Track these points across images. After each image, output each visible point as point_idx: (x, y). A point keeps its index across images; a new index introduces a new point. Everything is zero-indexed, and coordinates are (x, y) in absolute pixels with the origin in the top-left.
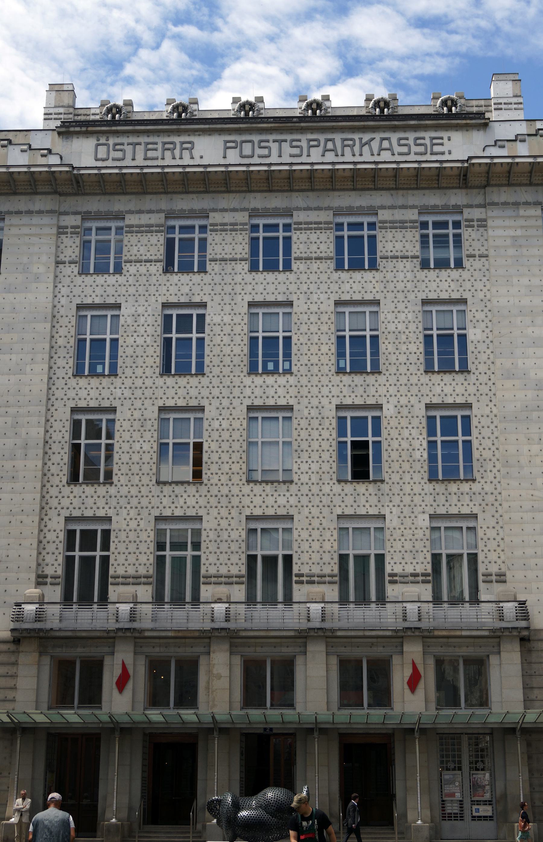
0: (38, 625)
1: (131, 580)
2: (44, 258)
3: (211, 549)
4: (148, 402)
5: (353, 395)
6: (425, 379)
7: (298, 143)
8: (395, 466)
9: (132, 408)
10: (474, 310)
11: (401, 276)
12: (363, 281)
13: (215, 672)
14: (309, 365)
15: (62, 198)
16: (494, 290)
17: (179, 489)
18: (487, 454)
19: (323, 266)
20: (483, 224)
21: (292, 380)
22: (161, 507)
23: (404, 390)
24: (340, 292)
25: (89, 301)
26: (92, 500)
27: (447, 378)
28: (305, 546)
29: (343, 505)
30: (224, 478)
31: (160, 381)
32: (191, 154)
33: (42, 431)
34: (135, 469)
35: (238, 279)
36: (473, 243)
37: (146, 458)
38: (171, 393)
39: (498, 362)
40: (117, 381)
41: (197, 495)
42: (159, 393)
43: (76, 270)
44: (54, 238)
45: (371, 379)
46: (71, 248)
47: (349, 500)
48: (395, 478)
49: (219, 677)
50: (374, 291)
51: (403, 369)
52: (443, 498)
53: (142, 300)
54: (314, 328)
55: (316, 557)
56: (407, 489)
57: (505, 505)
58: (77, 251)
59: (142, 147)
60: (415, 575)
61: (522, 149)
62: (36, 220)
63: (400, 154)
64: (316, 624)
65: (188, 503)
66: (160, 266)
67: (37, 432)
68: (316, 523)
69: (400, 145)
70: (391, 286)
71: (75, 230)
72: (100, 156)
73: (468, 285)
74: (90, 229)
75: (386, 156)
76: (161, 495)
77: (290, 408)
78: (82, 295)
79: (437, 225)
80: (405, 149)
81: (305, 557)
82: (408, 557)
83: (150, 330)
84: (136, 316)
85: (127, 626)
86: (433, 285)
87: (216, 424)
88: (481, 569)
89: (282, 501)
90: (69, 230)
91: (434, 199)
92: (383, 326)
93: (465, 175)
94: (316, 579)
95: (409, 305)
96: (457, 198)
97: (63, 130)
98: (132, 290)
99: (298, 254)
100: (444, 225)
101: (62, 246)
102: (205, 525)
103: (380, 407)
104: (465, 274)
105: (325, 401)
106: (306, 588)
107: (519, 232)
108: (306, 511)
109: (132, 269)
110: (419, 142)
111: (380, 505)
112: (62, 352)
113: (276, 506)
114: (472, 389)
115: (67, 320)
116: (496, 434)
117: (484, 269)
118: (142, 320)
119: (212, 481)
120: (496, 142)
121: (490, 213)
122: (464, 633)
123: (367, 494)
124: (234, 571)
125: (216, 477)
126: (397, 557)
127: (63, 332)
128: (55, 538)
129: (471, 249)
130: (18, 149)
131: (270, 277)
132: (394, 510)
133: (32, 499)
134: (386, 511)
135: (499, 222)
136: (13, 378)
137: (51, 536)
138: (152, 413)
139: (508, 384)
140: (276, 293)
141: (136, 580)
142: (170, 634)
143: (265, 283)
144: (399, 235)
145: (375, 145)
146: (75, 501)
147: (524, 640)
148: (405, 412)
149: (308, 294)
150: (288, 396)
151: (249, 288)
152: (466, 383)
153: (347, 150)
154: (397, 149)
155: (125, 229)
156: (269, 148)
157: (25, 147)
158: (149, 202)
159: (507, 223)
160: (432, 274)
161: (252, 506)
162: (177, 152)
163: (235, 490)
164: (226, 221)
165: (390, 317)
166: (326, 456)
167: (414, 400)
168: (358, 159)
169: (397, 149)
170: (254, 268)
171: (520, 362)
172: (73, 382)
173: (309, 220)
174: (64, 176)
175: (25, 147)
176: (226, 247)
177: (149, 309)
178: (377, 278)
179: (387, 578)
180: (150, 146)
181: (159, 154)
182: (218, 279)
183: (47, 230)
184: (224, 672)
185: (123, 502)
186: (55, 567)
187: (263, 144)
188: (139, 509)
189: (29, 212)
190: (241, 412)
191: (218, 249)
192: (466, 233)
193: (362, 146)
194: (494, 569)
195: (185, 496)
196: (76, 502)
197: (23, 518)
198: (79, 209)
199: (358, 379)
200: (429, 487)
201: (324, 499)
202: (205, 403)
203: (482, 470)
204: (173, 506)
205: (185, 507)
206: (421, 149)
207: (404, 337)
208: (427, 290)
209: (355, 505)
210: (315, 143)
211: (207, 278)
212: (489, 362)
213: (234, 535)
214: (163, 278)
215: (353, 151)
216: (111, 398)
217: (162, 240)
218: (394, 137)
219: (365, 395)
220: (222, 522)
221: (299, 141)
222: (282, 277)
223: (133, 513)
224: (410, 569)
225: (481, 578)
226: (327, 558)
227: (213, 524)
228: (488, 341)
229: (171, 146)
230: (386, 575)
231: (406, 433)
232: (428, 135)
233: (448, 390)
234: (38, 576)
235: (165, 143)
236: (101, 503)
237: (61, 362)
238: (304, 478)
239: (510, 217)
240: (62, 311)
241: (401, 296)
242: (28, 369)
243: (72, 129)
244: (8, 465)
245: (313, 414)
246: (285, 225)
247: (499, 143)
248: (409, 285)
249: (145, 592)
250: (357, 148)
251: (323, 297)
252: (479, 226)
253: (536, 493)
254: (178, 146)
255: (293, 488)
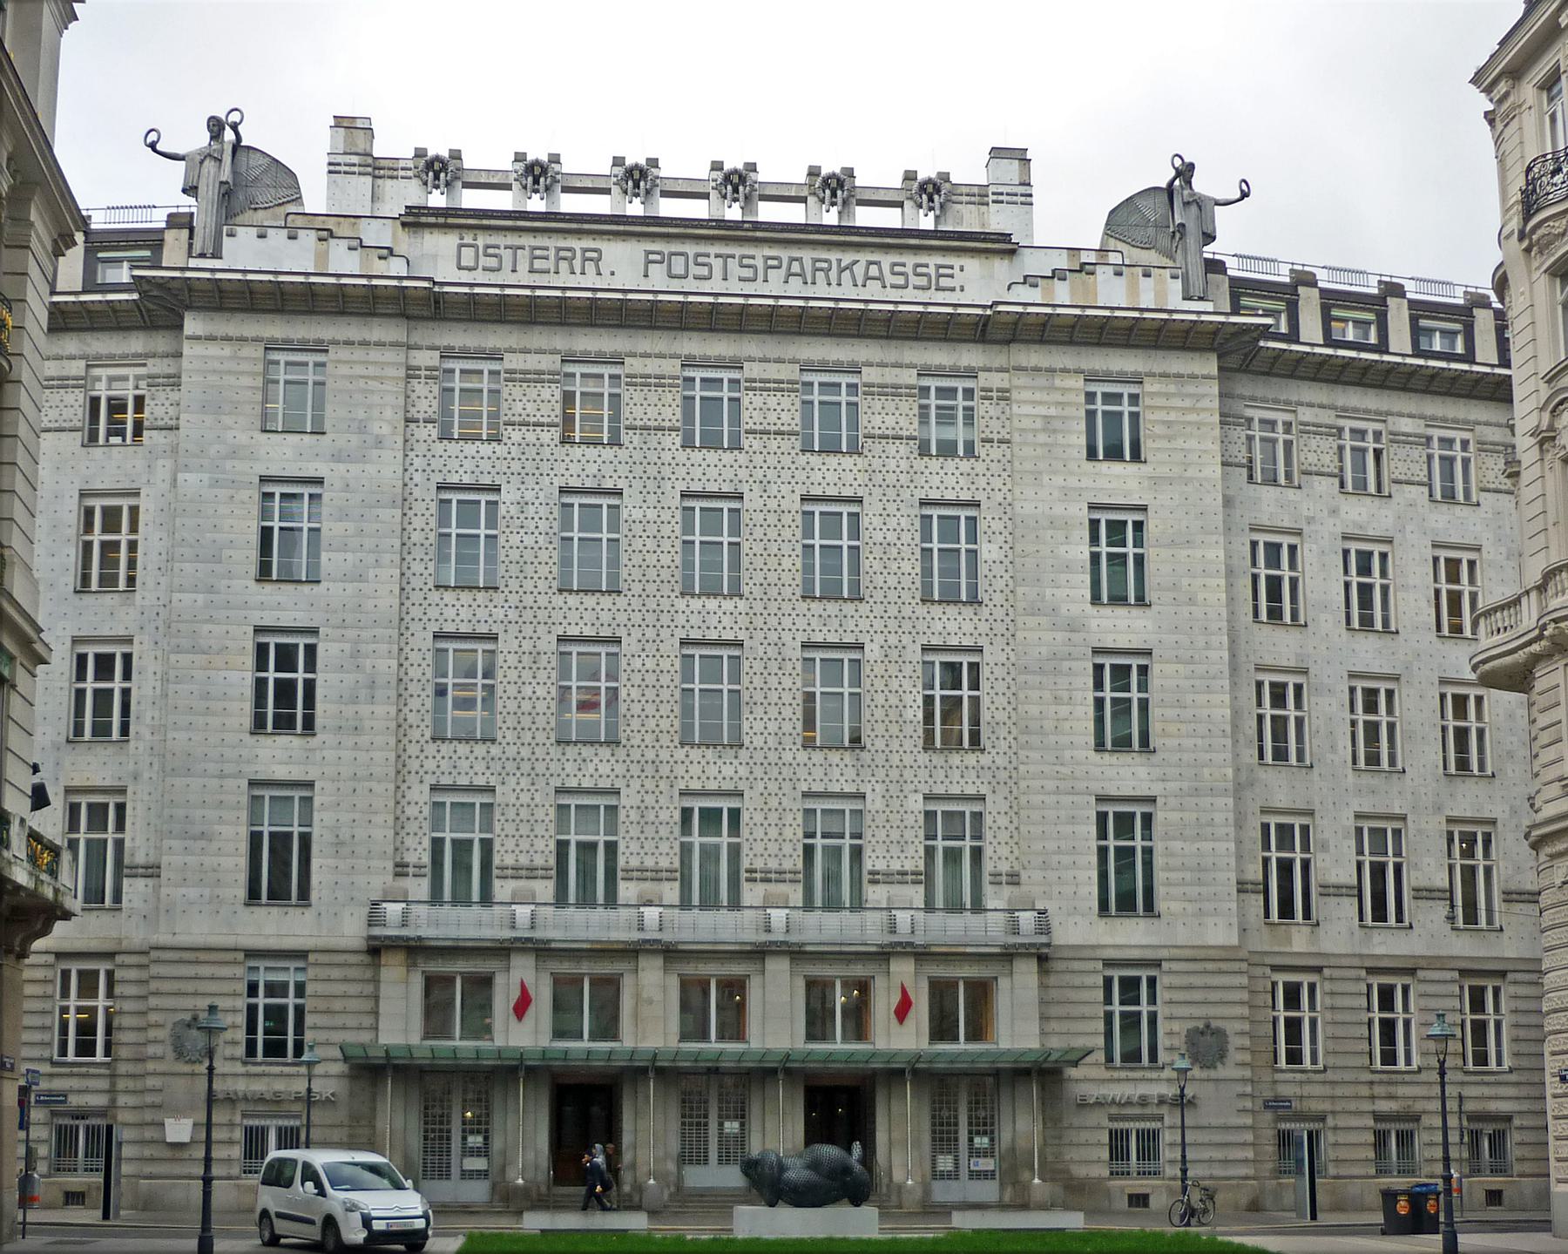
0: (404, 932)
1: (524, 873)
2: (388, 413)
3: (632, 834)
4: (541, 629)
5: (825, 630)
6: (921, 610)
7: (751, 262)
8: (880, 729)
9: (520, 636)
10: (989, 518)
11: (892, 464)
12: (840, 469)
13: (645, 995)
14: (765, 586)
15: (412, 323)
16: (1017, 491)
17: (587, 751)
18: (1001, 716)
19: (786, 444)
20: (1004, 395)
21: (742, 605)
22: (563, 775)
23: (893, 625)
24: (808, 482)
25: (455, 479)
26: (468, 763)
27: (952, 610)
28: (759, 833)
29: (810, 779)
30: (649, 738)
31: (558, 600)
32: (597, 267)
33: (394, 663)
34: (526, 722)
35: (667, 456)
36: (991, 423)
37: (541, 707)
38: (573, 616)
39: (1020, 590)
40: (498, 598)
41: (613, 760)
42: (557, 616)
43: (435, 434)
44: (402, 384)
45: (849, 608)
46: (426, 399)
47: (818, 773)
48: (880, 744)
49: (650, 1002)
50: (856, 484)
51: (892, 596)
52: (942, 773)
53: (530, 481)
54: (772, 534)
55: (773, 848)
56: (895, 759)
57: (1023, 784)
58: (435, 403)
59: (527, 252)
60: (904, 873)
61: (1062, 293)
62: (375, 354)
63: (893, 286)
64: (778, 936)
65: (601, 771)
66: (556, 433)
67: (386, 666)
68: (773, 802)
69: (894, 274)
70: (878, 478)
71: (433, 374)
72: (463, 264)
73: (982, 482)
74: (452, 371)
75: (873, 291)
76: (563, 759)
77: (739, 644)
78: (445, 470)
79: (943, 392)
80: (900, 281)
81: (759, 848)
82: (895, 850)
83: (543, 526)
84: (522, 505)
85: (527, 935)
86: (935, 481)
87: (637, 663)
88: (988, 866)
89: (728, 771)
90: (423, 373)
91: (938, 356)
92: (867, 534)
93: (985, 325)
94: (773, 876)
95: (902, 506)
96: (970, 356)
97: (410, 219)
98: (516, 466)
99: (751, 426)
100: (949, 393)
101: (414, 396)
102: (624, 801)
103: (861, 647)
104: (980, 467)
105: (787, 637)
106: (760, 888)
107: (1053, 411)
108: (761, 785)
109: (516, 435)
110: (919, 270)
111: (858, 780)
112: (418, 553)
113: (720, 778)
114: (983, 627)
115: (424, 505)
116: (1013, 689)
117: (1004, 460)
118: (531, 510)
119: (633, 742)
120: (1026, 277)
121: (1016, 382)
122: (969, 950)
123: (842, 765)
124: (664, 863)
125: (639, 737)
126: (880, 851)
127: (418, 522)
128: (416, 813)
129: (987, 431)
130: (344, 244)
131: (712, 456)
132: (878, 787)
133: (383, 759)
134: (866, 789)
135: (1026, 395)
136: (350, 587)
137: (411, 811)
138: (548, 644)
139: (1032, 621)
140: (720, 480)
141: (531, 873)
142: (585, 946)
143: (704, 464)
144: (890, 406)
145: (859, 270)
146: (445, 764)
147: (1042, 959)
148: (894, 654)
149: (764, 484)
150: (736, 628)
151: (681, 472)
152: (976, 619)
153: (820, 275)
154: (890, 279)
155: (503, 375)
156: (709, 266)
157: (355, 243)
158: (538, 338)
159: (1038, 396)
160: (935, 464)
161: (687, 777)
162: (577, 263)
163: (665, 755)
164: (648, 371)
165: (877, 521)
166: (787, 712)
167: (906, 639)
168: (835, 292)
169: (890, 279)
170: (688, 444)
171: (1048, 592)
172: (435, 596)
173: (765, 376)
174: (421, 293)
175: (355, 243)
176: (649, 410)
177: (541, 494)
178: (859, 467)
179: (866, 877)
180: (538, 253)
181: (550, 264)
182: (638, 456)
183: (391, 372)
184: (657, 996)
185: (510, 766)
186: (420, 854)
187: (700, 260)
188: (533, 776)
189: (364, 343)
190: (671, 647)
191: (638, 412)
192: (982, 408)
193: (841, 271)
194: (1004, 867)
195: (596, 760)
196: (445, 764)
197: (374, 785)
198: (437, 343)
199: (832, 608)
200: (923, 758)
201: (785, 770)
202: (621, 632)
203: (993, 738)
204: (580, 775)
205: (596, 775)
206: (923, 281)
207: (894, 551)
208: (927, 486)
209: (826, 780)
210: (775, 263)
211: (623, 454)
212: (1007, 591)
213: (664, 815)
214: (560, 452)
215: (827, 277)
216: (491, 621)
217: (558, 395)
218: (887, 260)
219: (841, 631)
220: (646, 798)
221: (753, 257)
222: (728, 457)
223: (524, 782)
224: (896, 866)
225: (986, 878)
226: (787, 848)
227: (635, 801)
228: (1006, 561)
229: (569, 254)
230: (865, 872)
231: (894, 684)
232: (933, 260)
233: (952, 626)
234: (397, 865)
235: (559, 249)
236: (480, 767)
237: (417, 567)
238: (758, 741)
239: (1041, 389)
240: (417, 493)
241: (891, 493)
242: (371, 573)
243: (423, 220)
244: (349, 710)
245: (770, 655)
246: (731, 381)
247: (1030, 280)
248: (903, 477)
249: (545, 889)
250: (833, 274)
251: (785, 489)
252: (999, 399)
253: (1063, 770)
254: (578, 254)
255: (743, 753)
